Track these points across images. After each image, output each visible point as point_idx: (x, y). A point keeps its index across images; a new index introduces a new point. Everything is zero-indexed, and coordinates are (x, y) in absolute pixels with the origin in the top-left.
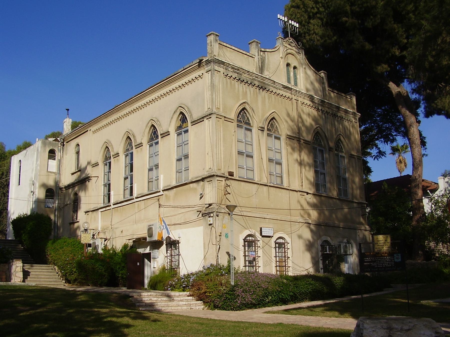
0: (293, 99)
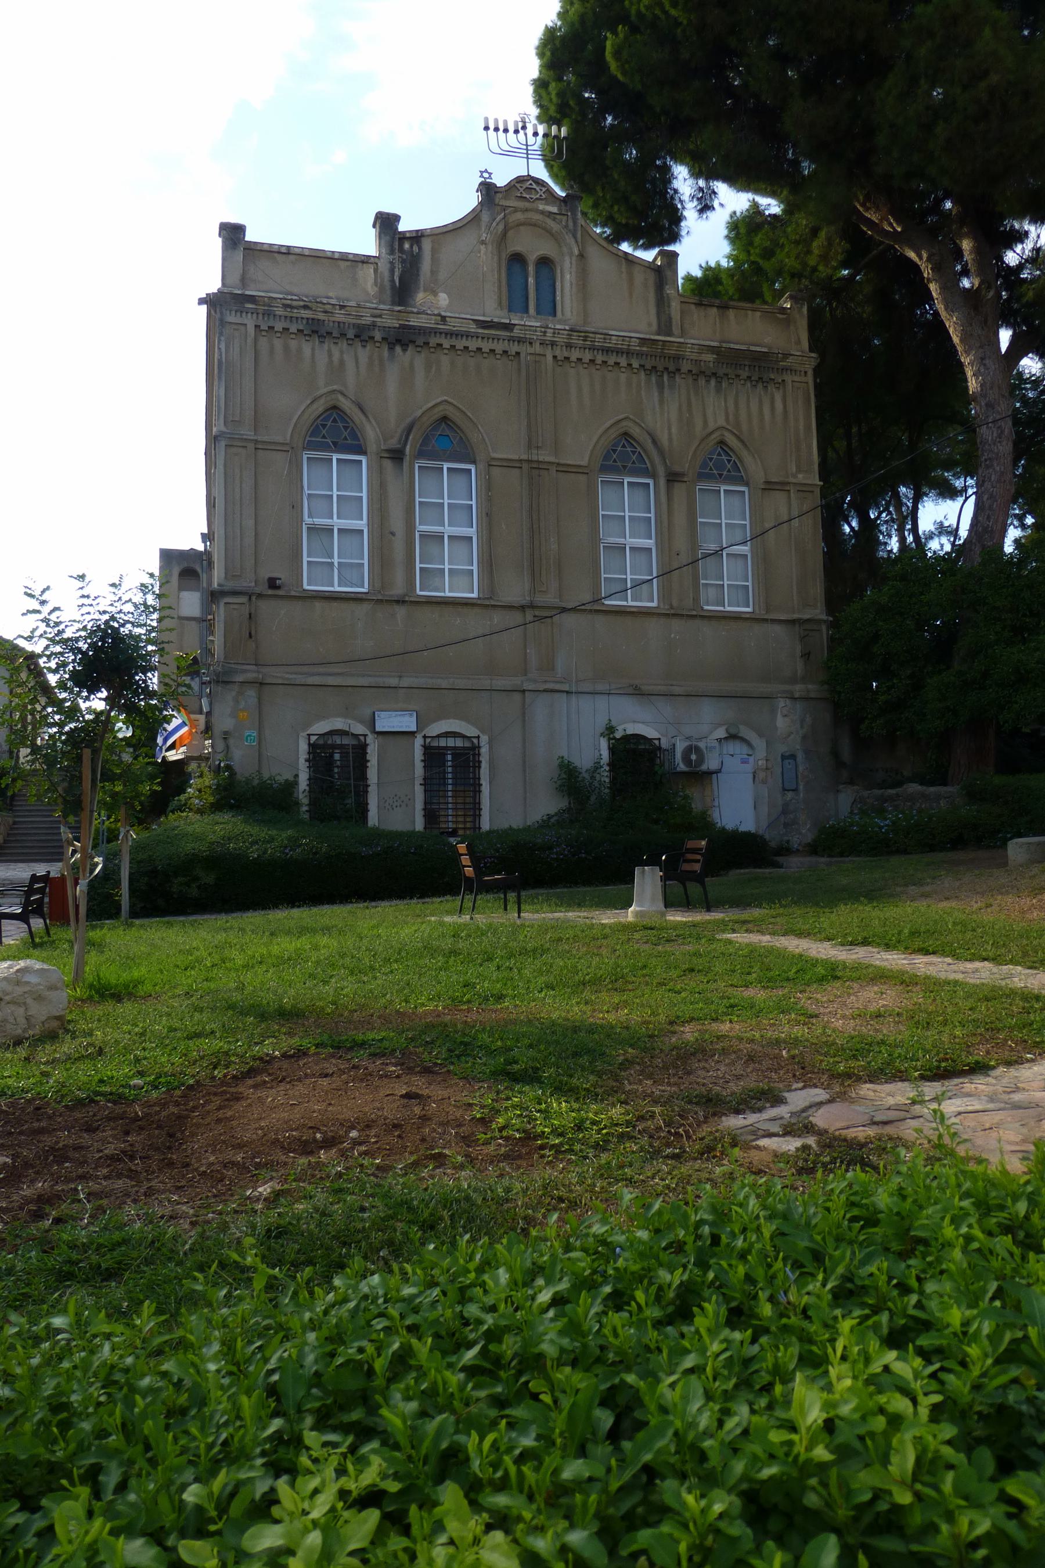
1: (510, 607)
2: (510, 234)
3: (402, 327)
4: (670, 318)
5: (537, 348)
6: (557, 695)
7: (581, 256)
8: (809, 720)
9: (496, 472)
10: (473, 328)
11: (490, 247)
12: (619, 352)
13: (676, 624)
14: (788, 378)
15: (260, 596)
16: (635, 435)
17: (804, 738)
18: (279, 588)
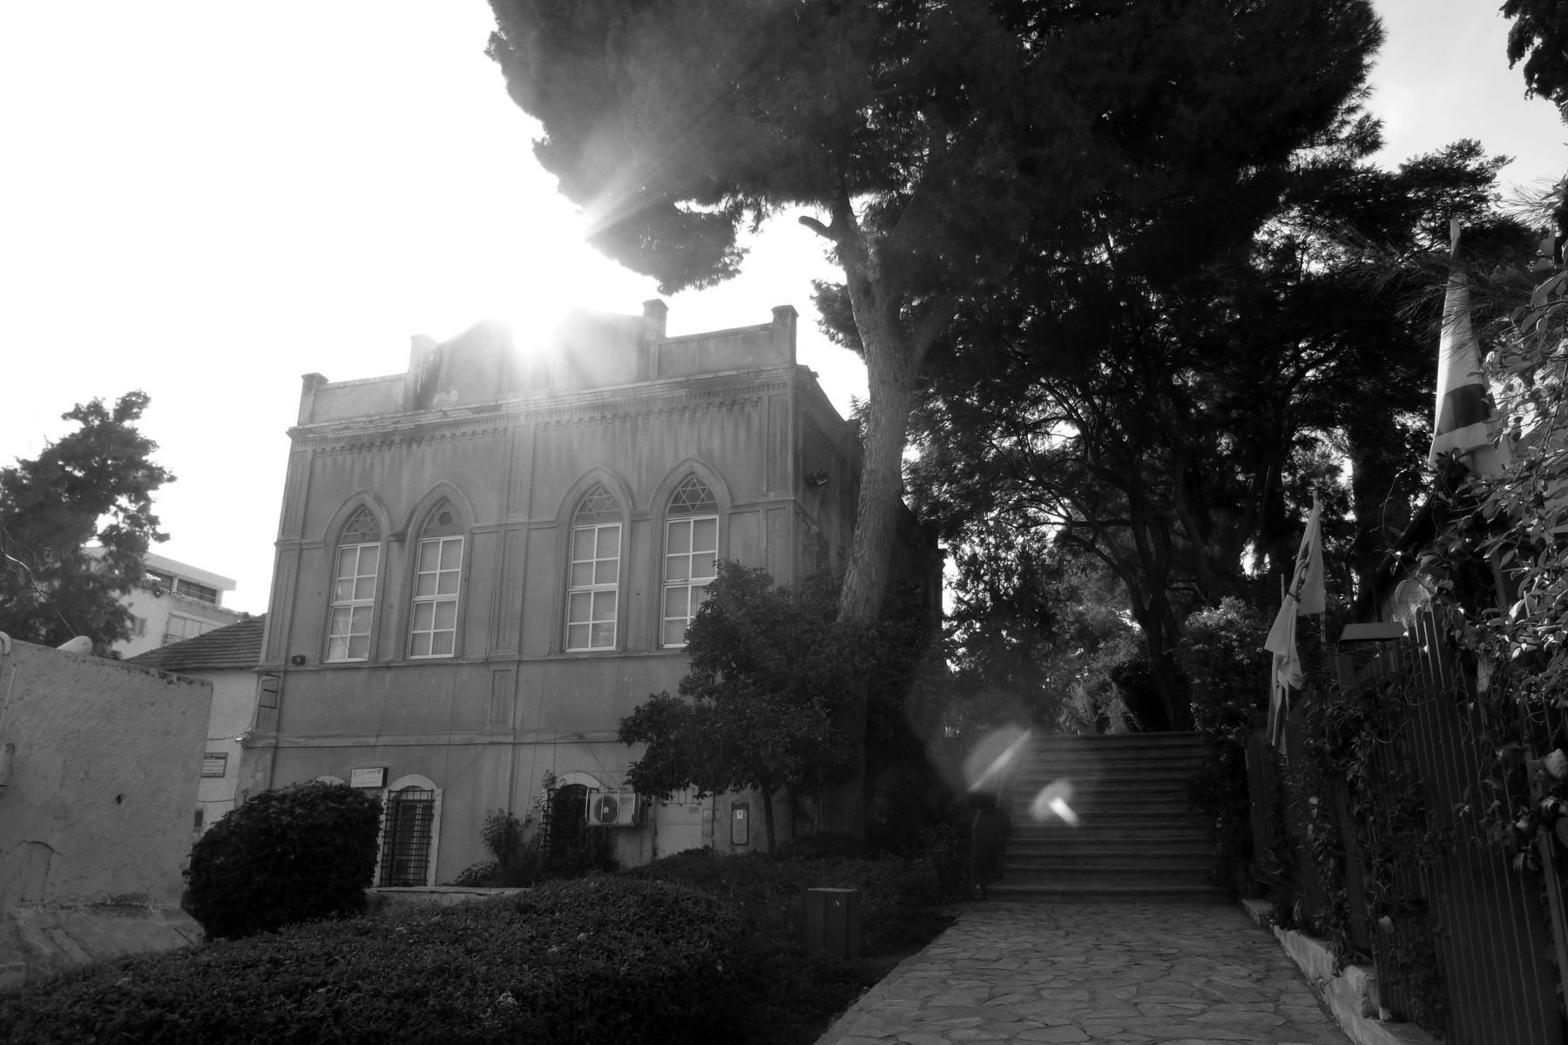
6: (503, 748)
10: (470, 416)
13: (630, 667)
14: (764, 394)
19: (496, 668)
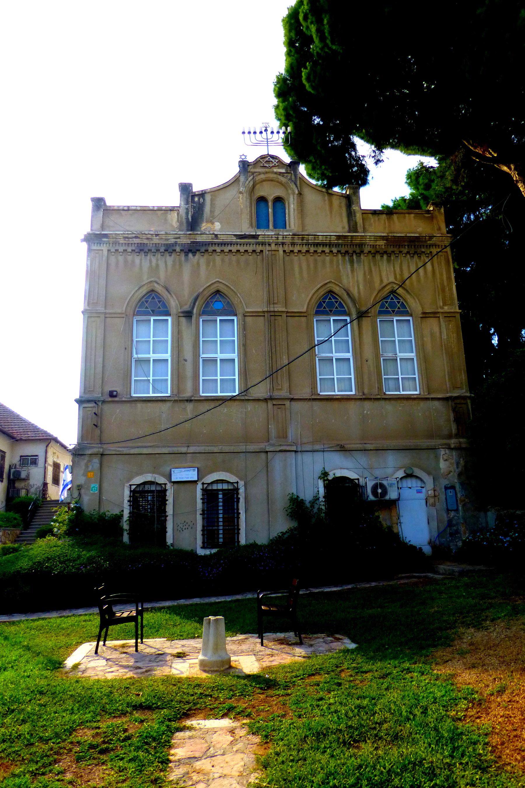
0: (266, 253)
1: (259, 400)
2: (257, 187)
3: (193, 243)
4: (356, 223)
5: (273, 247)
6: (289, 453)
7: (300, 194)
8: (462, 462)
9: (249, 319)
10: (234, 239)
11: (245, 195)
12: (324, 245)
13: (367, 404)
15: (104, 402)
16: (336, 291)
17: (460, 475)
18: (116, 396)
19: (275, 402)
